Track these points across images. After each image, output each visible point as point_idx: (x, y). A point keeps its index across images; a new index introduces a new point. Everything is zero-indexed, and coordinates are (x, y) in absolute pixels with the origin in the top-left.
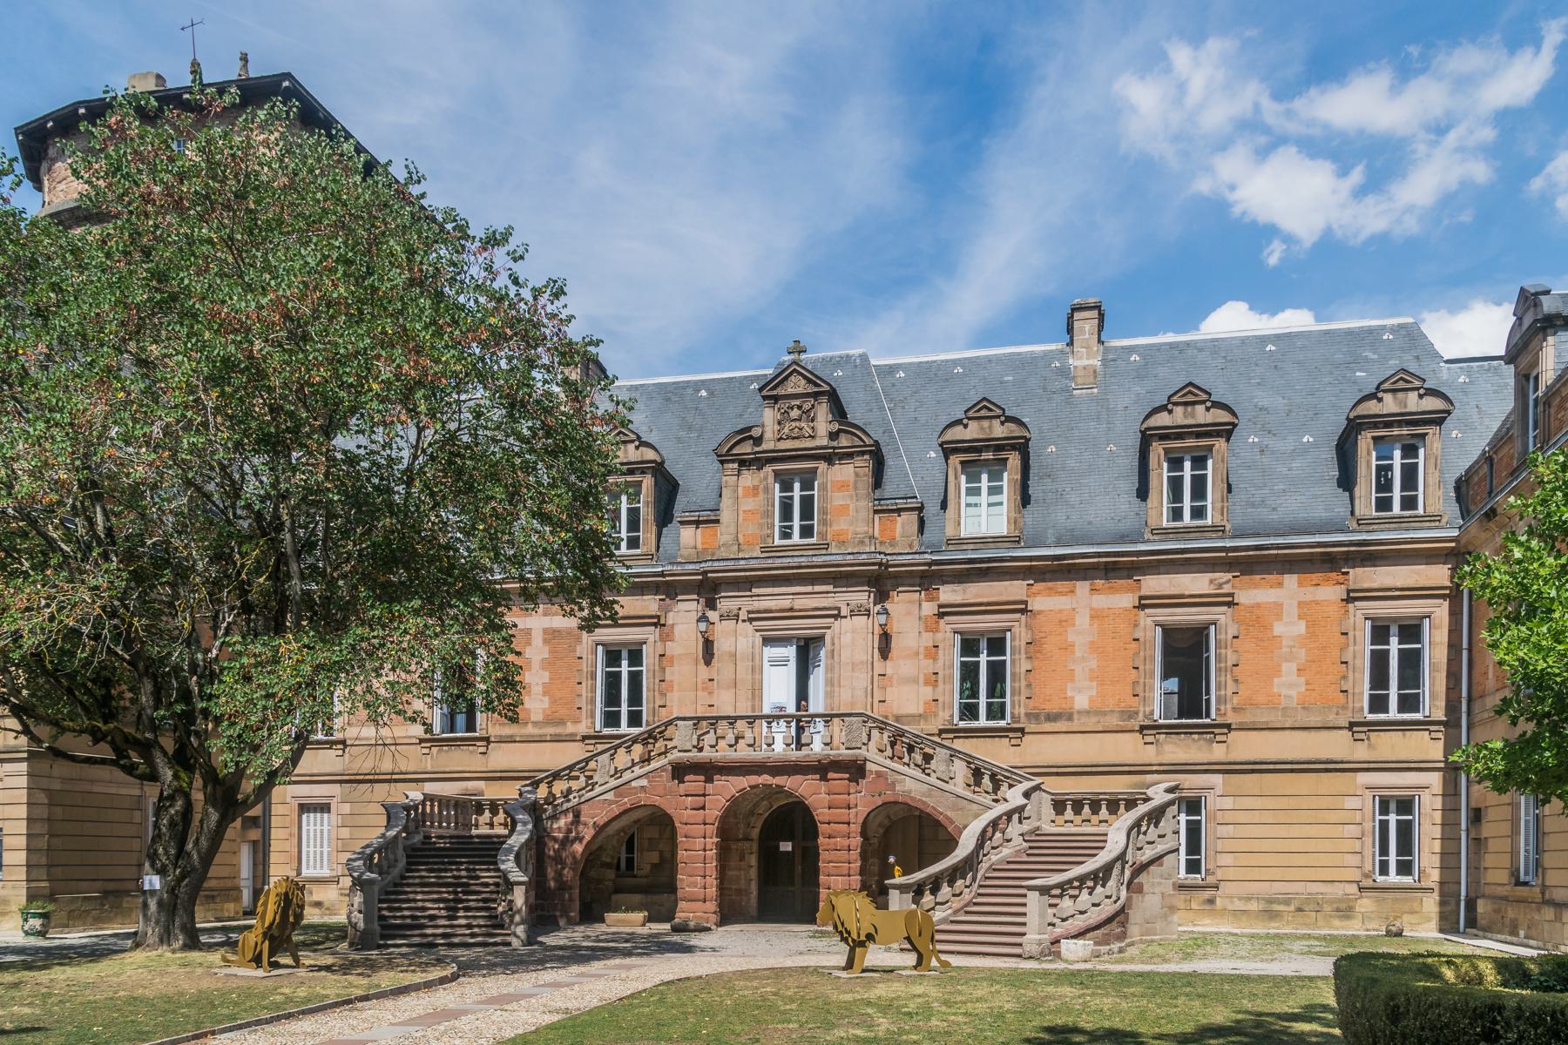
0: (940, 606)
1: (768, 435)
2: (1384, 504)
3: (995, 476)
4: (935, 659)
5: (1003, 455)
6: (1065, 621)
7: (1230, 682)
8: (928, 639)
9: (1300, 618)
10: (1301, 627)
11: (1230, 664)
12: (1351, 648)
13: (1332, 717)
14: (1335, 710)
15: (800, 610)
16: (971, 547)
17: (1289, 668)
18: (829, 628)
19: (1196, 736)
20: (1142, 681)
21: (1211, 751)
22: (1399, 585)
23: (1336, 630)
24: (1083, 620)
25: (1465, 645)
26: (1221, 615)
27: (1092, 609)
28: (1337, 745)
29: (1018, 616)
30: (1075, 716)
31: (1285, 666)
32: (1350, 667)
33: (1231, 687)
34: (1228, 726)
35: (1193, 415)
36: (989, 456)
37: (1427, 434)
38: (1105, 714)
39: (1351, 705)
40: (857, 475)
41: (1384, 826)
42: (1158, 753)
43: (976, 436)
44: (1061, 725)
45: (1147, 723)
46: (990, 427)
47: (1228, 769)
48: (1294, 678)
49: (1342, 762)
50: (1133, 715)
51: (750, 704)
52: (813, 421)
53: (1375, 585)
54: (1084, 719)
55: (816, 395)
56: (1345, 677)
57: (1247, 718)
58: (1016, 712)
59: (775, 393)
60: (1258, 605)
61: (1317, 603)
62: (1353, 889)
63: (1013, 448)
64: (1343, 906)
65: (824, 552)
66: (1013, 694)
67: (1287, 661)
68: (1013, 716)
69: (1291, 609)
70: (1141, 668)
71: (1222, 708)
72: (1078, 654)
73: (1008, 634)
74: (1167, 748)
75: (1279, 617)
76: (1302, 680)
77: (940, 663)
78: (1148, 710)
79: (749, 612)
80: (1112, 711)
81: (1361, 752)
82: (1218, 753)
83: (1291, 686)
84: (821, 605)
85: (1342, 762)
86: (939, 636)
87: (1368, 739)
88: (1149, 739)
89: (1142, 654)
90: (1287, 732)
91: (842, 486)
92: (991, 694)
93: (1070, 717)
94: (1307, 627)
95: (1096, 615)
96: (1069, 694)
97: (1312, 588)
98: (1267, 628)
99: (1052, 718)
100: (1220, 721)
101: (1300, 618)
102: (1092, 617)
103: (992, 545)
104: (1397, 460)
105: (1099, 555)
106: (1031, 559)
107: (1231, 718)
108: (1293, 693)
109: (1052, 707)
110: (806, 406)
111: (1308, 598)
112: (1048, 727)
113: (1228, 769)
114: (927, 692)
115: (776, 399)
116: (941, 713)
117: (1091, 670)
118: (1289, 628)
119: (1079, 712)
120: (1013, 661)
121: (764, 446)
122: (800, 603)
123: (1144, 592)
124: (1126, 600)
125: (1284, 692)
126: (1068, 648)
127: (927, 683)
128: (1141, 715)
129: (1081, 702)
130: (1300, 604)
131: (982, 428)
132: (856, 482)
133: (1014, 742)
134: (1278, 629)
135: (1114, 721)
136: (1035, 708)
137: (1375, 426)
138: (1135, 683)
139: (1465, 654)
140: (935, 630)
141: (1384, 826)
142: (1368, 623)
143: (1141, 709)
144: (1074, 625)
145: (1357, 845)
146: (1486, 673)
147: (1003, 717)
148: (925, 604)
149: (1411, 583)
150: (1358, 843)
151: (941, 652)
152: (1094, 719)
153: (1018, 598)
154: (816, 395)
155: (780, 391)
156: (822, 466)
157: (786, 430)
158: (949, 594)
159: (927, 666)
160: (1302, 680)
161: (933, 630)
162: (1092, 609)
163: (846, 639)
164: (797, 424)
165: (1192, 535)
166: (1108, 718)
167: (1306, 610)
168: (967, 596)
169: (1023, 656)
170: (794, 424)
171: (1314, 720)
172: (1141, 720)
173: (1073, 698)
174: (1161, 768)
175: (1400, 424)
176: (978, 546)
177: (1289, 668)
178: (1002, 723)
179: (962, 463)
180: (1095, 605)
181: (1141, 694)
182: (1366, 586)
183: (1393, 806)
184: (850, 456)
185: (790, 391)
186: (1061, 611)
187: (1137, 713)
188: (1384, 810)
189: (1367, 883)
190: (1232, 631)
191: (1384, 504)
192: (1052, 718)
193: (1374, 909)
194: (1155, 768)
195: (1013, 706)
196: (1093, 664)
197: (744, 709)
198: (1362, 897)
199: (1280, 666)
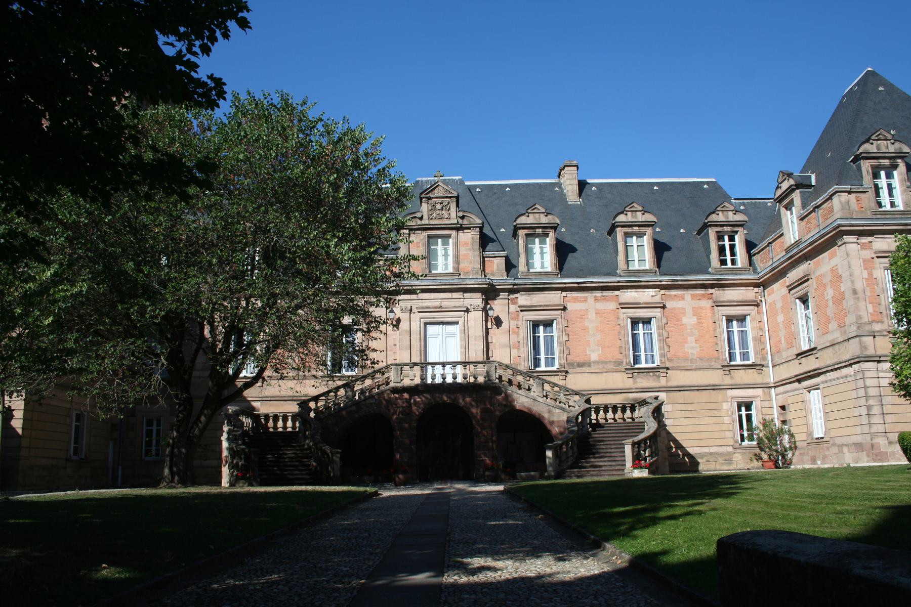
0: (519, 307)
1: (425, 217)
2: (723, 262)
3: (543, 242)
4: (518, 335)
5: (547, 231)
6: (583, 315)
7: (665, 346)
8: (513, 324)
9: (694, 315)
10: (694, 320)
11: (664, 337)
12: (718, 330)
13: (713, 363)
14: (714, 360)
15: (446, 308)
16: (534, 277)
17: (691, 339)
18: (461, 317)
19: (651, 374)
20: (623, 346)
21: (659, 381)
22: (735, 299)
23: (711, 321)
24: (592, 315)
25: (767, 329)
26: (657, 312)
27: (596, 309)
28: (715, 377)
29: (559, 312)
30: (592, 364)
31: (689, 338)
32: (719, 339)
33: (666, 349)
34: (668, 369)
35: (636, 217)
36: (539, 231)
37: (738, 231)
38: (606, 363)
39: (721, 357)
40: (473, 238)
41: (740, 417)
42: (634, 383)
43: (532, 222)
44: (585, 369)
45: (628, 367)
46: (539, 218)
47: (668, 390)
48: (693, 344)
49: (720, 386)
50: (620, 363)
51: (419, 358)
52: (448, 210)
53: (725, 299)
54: (596, 366)
55: (450, 197)
56: (717, 344)
57: (675, 364)
58: (562, 362)
59: (428, 196)
60: (674, 309)
61: (701, 308)
62: (730, 449)
63: (551, 228)
64: (727, 458)
65: (457, 277)
66: (560, 352)
67: (690, 336)
68: (560, 365)
69: (689, 311)
70: (622, 339)
71: (663, 359)
72: (591, 332)
73: (555, 322)
74: (639, 380)
75: (684, 314)
76: (698, 345)
77: (521, 337)
78: (628, 360)
79: (417, 308)
80: (610, 362)
81: (727, 381)
82: (663, 382)
83: (693, 348)
84: (457, 305)
85: (720, 386)
86: (520, 323)
87: (730, 374)
88: (630, 375)
89: (622, 332)
90: (694, 372)
91: (465, 244)
92: (546, 354)
93: (589, 365)
94: (697, 319)
95: (598, 313)
96: (588, 353)
97: (698, 301)
98: (680, 320)
99: (580, 365)
100: (663, 366)
101: (694, 315)
102: (597, 314)
103: (544, 276)
104: (727, 243)
105: (599, 282)
106: (565, 283)
107: (668, 365)
108: (694, 352)
109: (580, 359)
110: (445, 203)
111: (696, 306)
112: (578, 370)
113: (668, 390)
114: (514, 352)
115: (429, 198)
116: (523, 364)
117: (598, 340)
118: (689, 320)
119: (594, 362)
120: (559, 336)
121: (423, 222)
122: (445, 304)
123: (622, 301)
124: (612, 306)
125: (690, 351)
126: (586, 329)
127: (514, 348)
128: (624, 363)
129: (594, 357)
130: (693, 308)
131: (535, 218)
132: (473, 242)
133: (561, 378)
134: (685, 320)
135: (611, 366)
136: (571, 360)
137: (716, 226)
138: (621, 347)
139: (767, 332)
140: (517, 320)
141: (740, 417)
142: (724, 318)
143: (625, 360)
144: (588, 318)
145: (731, 427)
146: (780, 341)
147: (553, 366)
148: (510, 306)
149: (740, 298)
150: (731, 426)
151: (521, 331)
152: (601, 366)
153: (559, 303)
154: (450, 197)
155: (432, 196)
156: (454, 233)
157: (434, 215)
158: (523, 299)
159: (514, 338)
160: (698, 345)
161: (517, 320)
162: (596, 309)
163: (471, 323)
164: (440, 212)
165: (641, 274)
166: (608, 365)
167: (697, 312)
168: (533, 302)
169: (564, 333)
170: (438, 212)
171: (705, 365)
172: (625, 366)
173: (590, 355)
174: (637, 390)
175: (727, 225)
176: (537, 277)
177: (691, 339)
178: (554, 369)
179: (527, 235)
180: (597, 307)
181: (624, 353)
182: (722, 299)
183: (743, 409)
184: (469, 228)
185: (436, 195)
186: (581, 310)
187: (622, 362)
188: (739, 410)
189: (737, 445)
190: (664, 321)
191: (723, 262)
192: (580, 365)
193: (741, 458)
194: (633, 391)
195: (560, 359)
196: (599, 337)
197: (416, 359)
198: (735, 453)
199: (687, 338)
